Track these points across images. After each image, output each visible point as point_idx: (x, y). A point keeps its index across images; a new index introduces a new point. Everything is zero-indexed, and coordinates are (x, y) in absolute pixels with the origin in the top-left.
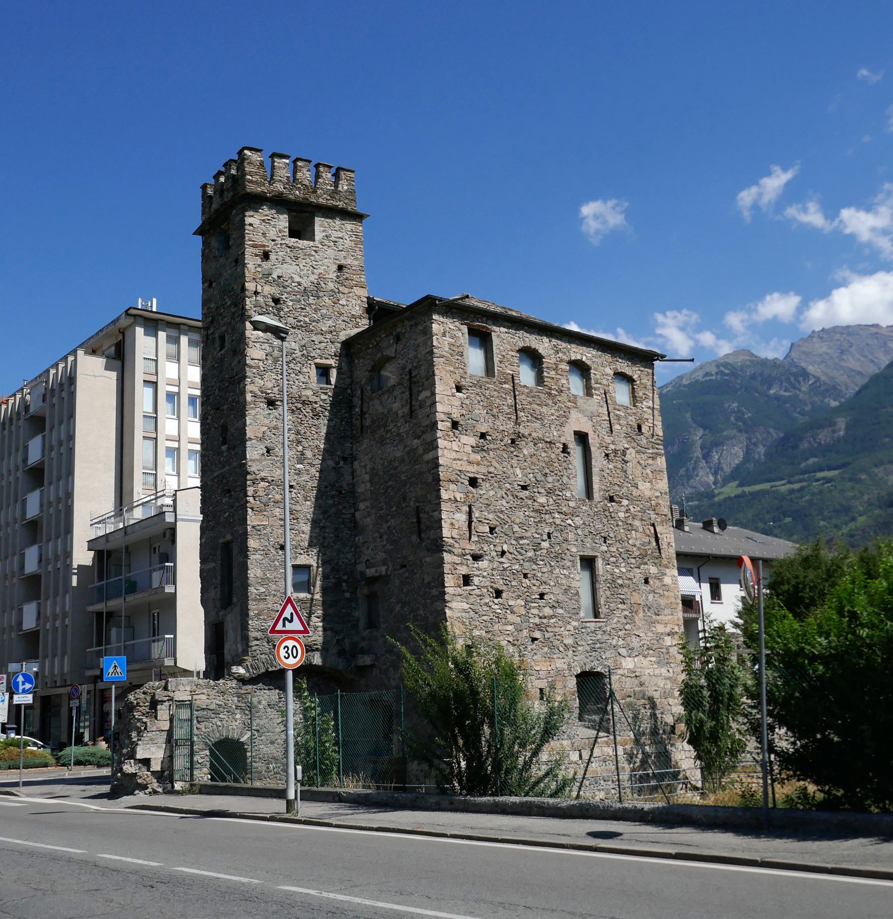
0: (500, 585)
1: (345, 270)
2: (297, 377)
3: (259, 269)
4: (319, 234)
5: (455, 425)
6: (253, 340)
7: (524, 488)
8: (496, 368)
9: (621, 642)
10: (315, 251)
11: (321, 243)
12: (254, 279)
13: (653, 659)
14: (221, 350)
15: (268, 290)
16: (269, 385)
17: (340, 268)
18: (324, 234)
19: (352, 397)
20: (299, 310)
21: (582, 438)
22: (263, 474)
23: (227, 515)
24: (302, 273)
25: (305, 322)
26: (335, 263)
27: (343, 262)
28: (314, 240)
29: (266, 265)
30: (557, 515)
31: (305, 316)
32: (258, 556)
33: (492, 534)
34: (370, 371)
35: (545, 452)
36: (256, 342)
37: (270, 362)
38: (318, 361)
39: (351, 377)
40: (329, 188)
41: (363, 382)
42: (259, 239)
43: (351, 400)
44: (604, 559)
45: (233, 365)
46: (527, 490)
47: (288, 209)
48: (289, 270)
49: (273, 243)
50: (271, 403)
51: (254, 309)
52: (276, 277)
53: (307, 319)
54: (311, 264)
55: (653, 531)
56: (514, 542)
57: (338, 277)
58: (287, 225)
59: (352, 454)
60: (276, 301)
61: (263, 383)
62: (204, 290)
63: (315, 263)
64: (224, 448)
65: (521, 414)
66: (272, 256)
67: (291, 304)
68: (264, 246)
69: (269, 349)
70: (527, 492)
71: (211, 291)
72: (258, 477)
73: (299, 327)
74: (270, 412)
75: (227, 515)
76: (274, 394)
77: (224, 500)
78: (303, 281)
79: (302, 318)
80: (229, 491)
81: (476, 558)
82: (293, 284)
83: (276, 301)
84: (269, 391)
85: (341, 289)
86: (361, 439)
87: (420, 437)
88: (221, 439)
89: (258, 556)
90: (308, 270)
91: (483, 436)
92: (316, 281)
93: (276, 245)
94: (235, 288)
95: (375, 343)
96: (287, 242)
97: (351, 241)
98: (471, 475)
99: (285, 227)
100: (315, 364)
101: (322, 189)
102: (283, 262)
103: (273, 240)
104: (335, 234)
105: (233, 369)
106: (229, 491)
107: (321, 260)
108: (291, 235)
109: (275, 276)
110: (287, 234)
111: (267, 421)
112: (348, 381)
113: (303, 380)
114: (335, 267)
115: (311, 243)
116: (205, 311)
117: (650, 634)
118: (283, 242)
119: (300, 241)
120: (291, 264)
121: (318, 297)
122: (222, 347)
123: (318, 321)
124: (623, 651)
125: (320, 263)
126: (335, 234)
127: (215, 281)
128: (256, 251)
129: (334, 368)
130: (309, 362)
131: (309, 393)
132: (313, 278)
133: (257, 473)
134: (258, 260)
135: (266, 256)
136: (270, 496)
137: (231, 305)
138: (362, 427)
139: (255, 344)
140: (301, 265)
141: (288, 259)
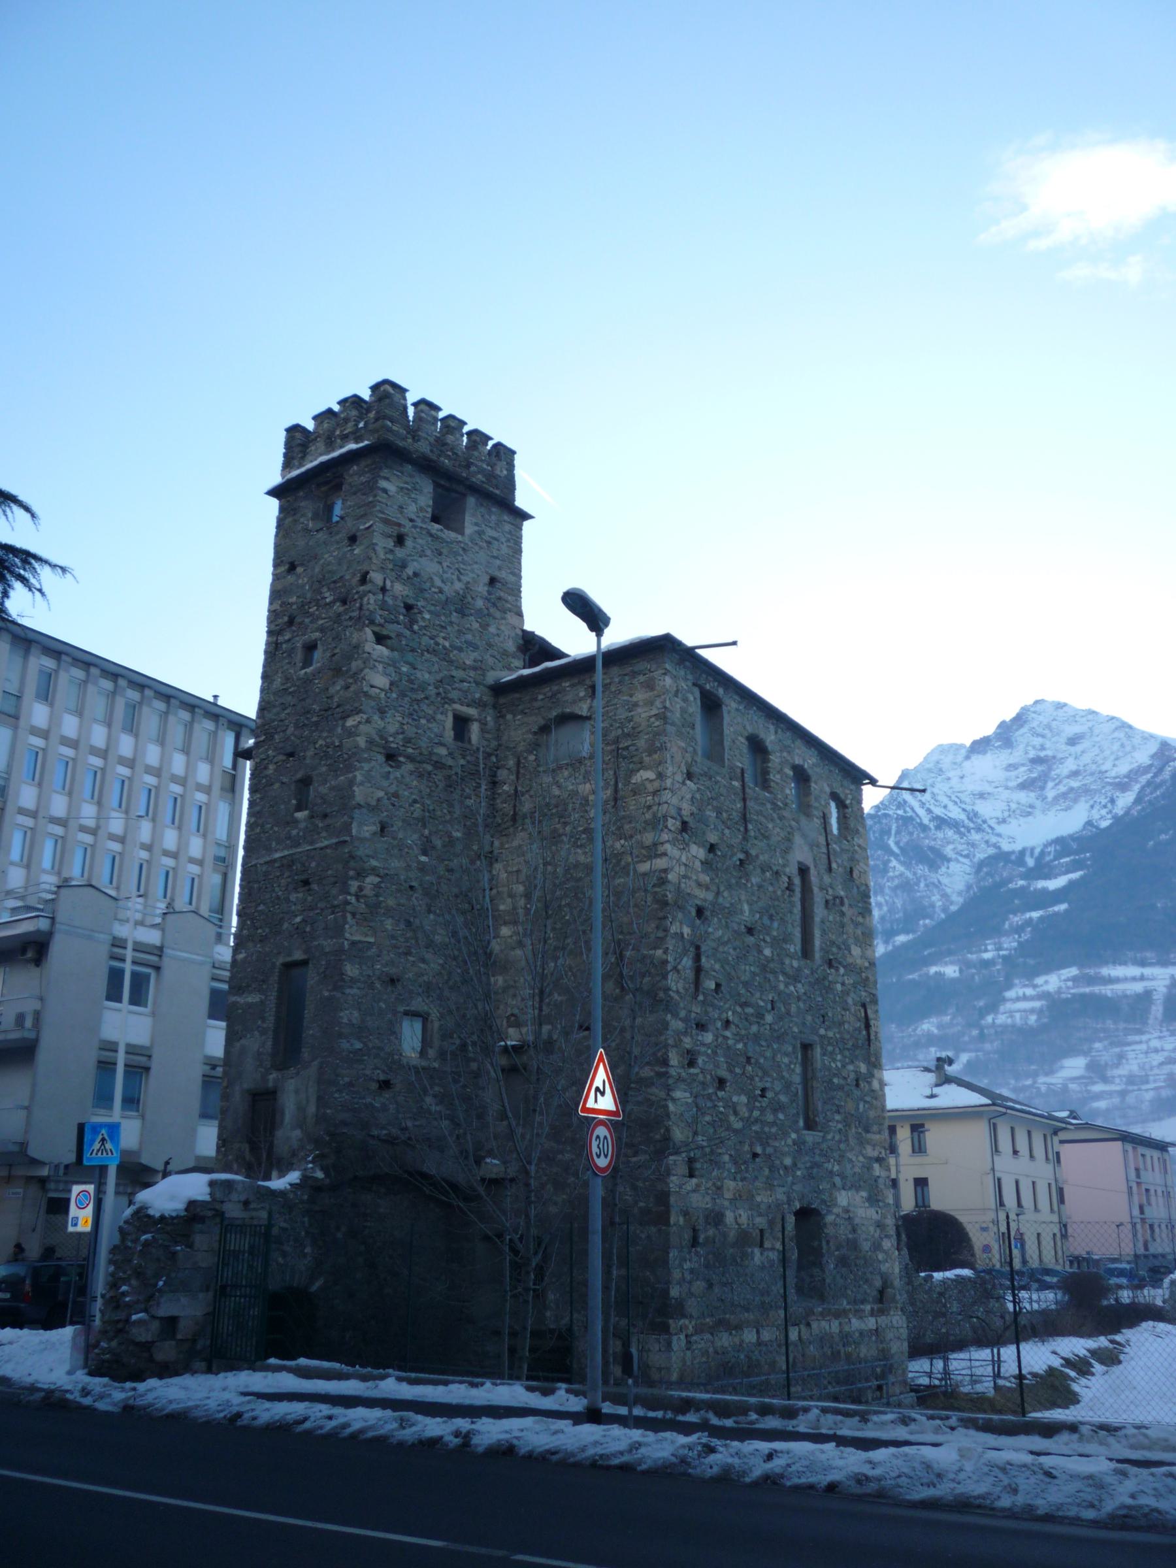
0: (723, 1073)
1: (498, 585)
2: (430, 725)
3: (391, 557)
4: (469, 529)
5: (685, 826)
7: (750, 931)
8: (726, 755)
9: (836, 1168)
10: (464, 549)
11: (472, 540)
12: (382, 568)
13: (864, 1194)
14: (303, 668)
15: (399, 588)
16: (392, 729)
18: (477, 528)
19: (498, 768)
20: (438, 628)
21: (803, 871)
22: (374, 863)
23: (298, 919)
24: (445, 576)
25: (444, 648)
28: (463, 534)
29: (400, 553)
30: (781, 978)
31: (444, 638)
32: (355, 991)
33: (717, 993)
34: (535, 733)
35: (772, 884)
36: (379, 662)
37: (394, 695)
38: (457, 706)
39: (498, 738)
40: (485, 466)
41: (520, 748)
42: (392, 513)
43: (496, 772)
44: (822, 1048)
45: (332, 690)
46: (752, 935)
47: (434, 481)
48: (429, 566)
49: (411, 524)
50: (390, 757)
52: (411, 573)
53: (447, 644)
54: (457, 566)
55: (863, 1015)
56: (739, 1009)
57: (489, 593)
58: (431, 503)
59: (491, 852)
60: (409, 607)
61: (383, 725)
62: (276, 577)
63: (462, 566)
64: (299, 815)
65: (750, 827)
66: (409, 543)
67: (427, 616)
68: (399, 525)
69: (395, 677)
70: (752, 939)
71: (290, 578)
72: (367, 866)
73: (434, 652)
74: (391, 770)
75: (298, 919)
76: (395, 743)
78: (446, 589)
79: (441, 641)
80: (306, 883)
81: (701, 1027)
82: (433, 589)
83: (409, 607)
84: (391, 739)
86: (511, 830)
87: (631, 837)
88: (294, 802)
89: (355, 991)
90: (452, 574)
91: (712, 848)
92: (461, 592)
93: (415, 527)
94: (347, 577)
95: (550, 694)
96: (429, 528)
97: (508, 546)
98: (699, 903)
99: (429, 506)
100: (454, 710)
101: (476, 466)
102: (422, 554)
103: (411, 520)
104: (490, 533)
105: (331, 697)
106: (306, 883)
107: (470, 565)
108: (435, 519)
109: (409, 571)
110: (429, 515)
111: (385, 783)
112: (494, 744)
113: (436, 730)
114: (486, 579)
115: (460, 538)
116: (276, 606)
117: (861, 1159)
118: (424, 526)
119: (445, 531)
120: (432, 560)
121: (464, 615)
122: (307, 662)
123: (460, 650)
124: (837, 1180)
125: (469, 568)
126: (490, 533)
127: (302, 565)
128: (388, 530)
129: (476, 720)
130: (446, 706)
131: (443, 751)
132: (458, 586)
133: (366, 859)
134: (390, 543)
135: (400, 540)
136: (381, 899)
137: (334, 602)
138: (515, 814)
139: (377, 664)
140: (445, 564)
141: (428, 552)
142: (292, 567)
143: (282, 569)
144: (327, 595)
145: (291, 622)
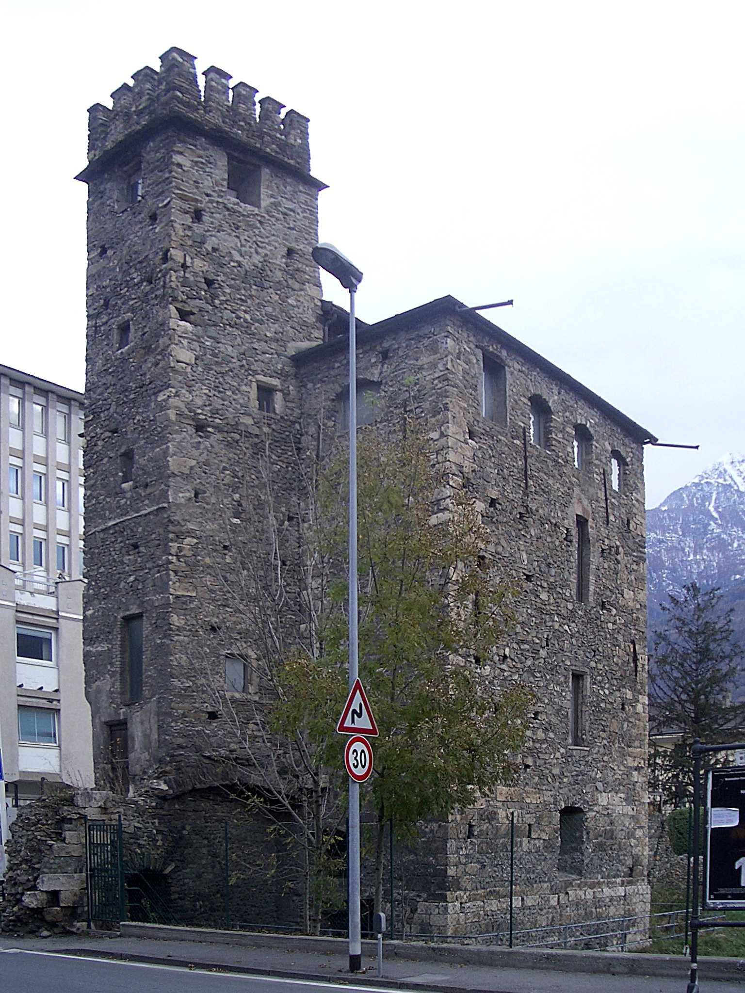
2: (235, 397)
3: (189, 233)
6: (179, 333)
7: (528, 578)
9: (599, 775)
10: (260, 222)
13: (623, 795)
15: (199, 264)
16: (199, 402)
17: (290, 252)
22: (191, 526)
23: (132, 578)
25: (246, 321)
26: (285, 245)
27: (294, 245)
28: (259, 207)
30: (556, 618)
31: (245, 312)
35: (550, 535)
38: (260, 377)
40: (278, 135)
42: (190, 190)
45: (144, 368)
47: (228, 154)
48: (225, 241)
50: (200, 428)
51: (183, 289)
52: (210, 249)
53: (248, 317)
54: (254, 239)
56: (515, 646)
58: (226, 177)
60: (209, 283)
63: (260, 239)
65: (531, 482)
66: (206, 218)
67: (228, 291)
68: (196, 200)
74: (201, 440)
75: (132, 578)
77: (126, 559)
78: (244, 262)
79: (242, 314)
80: (136, 546)
82: (232, 264)
83: (209, 283)
85: (290, 282)
90: (251, 247)
92: (260, 265)
93: (212, 202)
99: (224, 180)
100: (257, 381)
101: (270, 135)
106: (136, 546)
107: (267, 237)
111: (196, 453)
113: (241, 401)
115: (256, 211)
117: (622, 768)
118: (220, 200)
119: (242, 204)
120: (229, 234)
121: (263, 288)
124: (600, 785)
125: (266, 240)
128: (186, 206)
130: (250, 378)
134: (188, 220)
135: (198, 216)
137: (142, 281)
139: (181, 339)
140: (242, 238)
141: (226, 227)
142: (104, 251)
143: (95, 253)
144: (135, 275)
145: (106, 305)
